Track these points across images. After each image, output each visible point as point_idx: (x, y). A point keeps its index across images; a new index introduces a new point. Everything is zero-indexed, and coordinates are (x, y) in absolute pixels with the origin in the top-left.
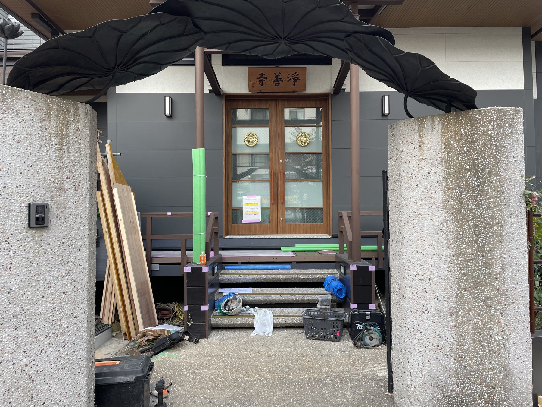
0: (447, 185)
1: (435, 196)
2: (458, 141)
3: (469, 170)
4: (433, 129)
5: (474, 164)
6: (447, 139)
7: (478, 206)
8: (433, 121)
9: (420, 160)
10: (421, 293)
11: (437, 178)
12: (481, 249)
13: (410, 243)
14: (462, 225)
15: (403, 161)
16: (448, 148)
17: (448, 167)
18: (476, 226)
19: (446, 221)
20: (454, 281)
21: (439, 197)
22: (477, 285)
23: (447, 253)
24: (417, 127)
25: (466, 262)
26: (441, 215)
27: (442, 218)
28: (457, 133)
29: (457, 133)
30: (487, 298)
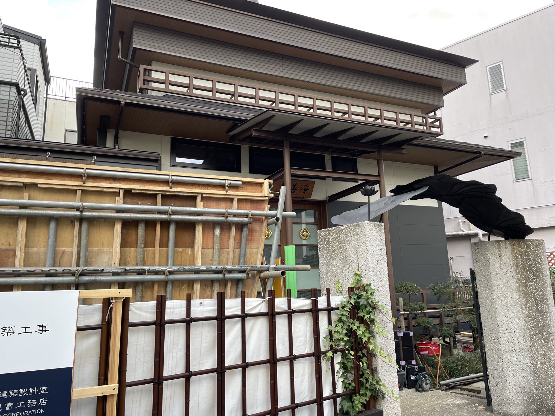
0: (518, 278)
1: (512, 284)
2: (521, 255)
3: (528, 271)
4: (506, 248)
5: (531, 267)
6: (515, 253)
7: (536, 290)
8: (506, 244)
9: (501, 264)
10: (510, 340)
11: (512, 274)
12: (540, 312)
13: (500, 311)
14: (528, 300)
15: (491, 264)
16: (516, 258)
17: (517, 269)
18: (536, 300)
19: (520, 298)
20: (528, 331)
21: (514, 285)
22: (540, 331)
23: (522, 316)
24: (497, 246)
25: (533, 320)
26: (516, 295)
27: (518, 297)
28: (520, 251)
29: (520, 251)
30: (546, 338)
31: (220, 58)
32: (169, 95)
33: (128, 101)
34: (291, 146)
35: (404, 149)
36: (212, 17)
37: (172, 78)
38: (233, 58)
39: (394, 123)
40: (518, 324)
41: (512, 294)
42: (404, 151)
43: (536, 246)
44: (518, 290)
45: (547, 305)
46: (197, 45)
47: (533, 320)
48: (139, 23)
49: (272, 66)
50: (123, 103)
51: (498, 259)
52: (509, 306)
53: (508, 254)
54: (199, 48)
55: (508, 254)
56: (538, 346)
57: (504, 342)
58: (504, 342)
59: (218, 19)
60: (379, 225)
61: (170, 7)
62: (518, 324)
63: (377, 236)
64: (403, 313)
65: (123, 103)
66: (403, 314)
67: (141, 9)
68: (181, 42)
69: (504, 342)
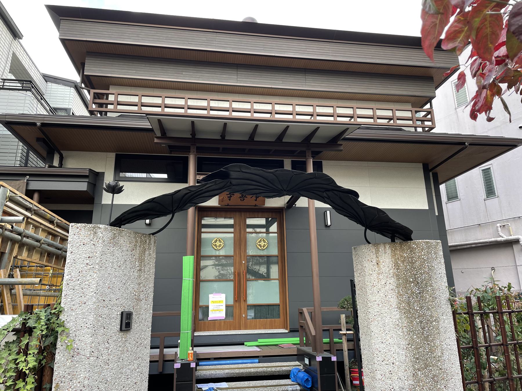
0: (399, 292)
1: (392, 300)
2: (403, 262)
3: (412, 282)
4: (385, 253)
5: (415, 278)
6: (395, 260)
7: (421, 308)
8: (385, 247)
9: (379, 274)
10: (388, 375)
11: (391, 287)
12: (426, 338)
13: (377, 335)
14: (412, 322)
15: (367, 274)
16: (397, 266)
17: (398, 279)
18: (421, 322)
19: (400, 318)
20: (410, 364)
21: (394, 301)
22: (426, 366)
23: (404, 343)
24: (374, 250)
25: (417, 349)
26: (396, 315)
27: (398, 316)
28: (402, 256)
29: (402, 256)
30: (434, 376)
31: (169, 74)
32: (124, 115)
33: (43, 122)
34: (199, 150)
35: (341, 145)
36: (155, 37)
37: (145, 100)
38: (184, 73)
39: (331, 119)
40: (398, 354)
41: (391, 313)
42: (342, 148)
43: (422, 250)
44: (399, 308)
45: (438, 329)
46: (146, 65)
47: (417, 349)
48: (92, 52)
49: (225, 76)
50: (38, 124)
51: (376, 266)
52: (387, 328)
53: (387, 260)
54: (148, 68)
55: (387, 260)
56: (423, 386)
57: (380, 377)
58: (380, 377)
59: (161, 38)
60: (94, 228)
61: (114, 34)
62: (398, 354)
63: (87, 240)
64: (345, 332)
65: (38, 124)
66: (345, 334)
67: (85, 39)
68: (131, 64)
69: (379, 377)
